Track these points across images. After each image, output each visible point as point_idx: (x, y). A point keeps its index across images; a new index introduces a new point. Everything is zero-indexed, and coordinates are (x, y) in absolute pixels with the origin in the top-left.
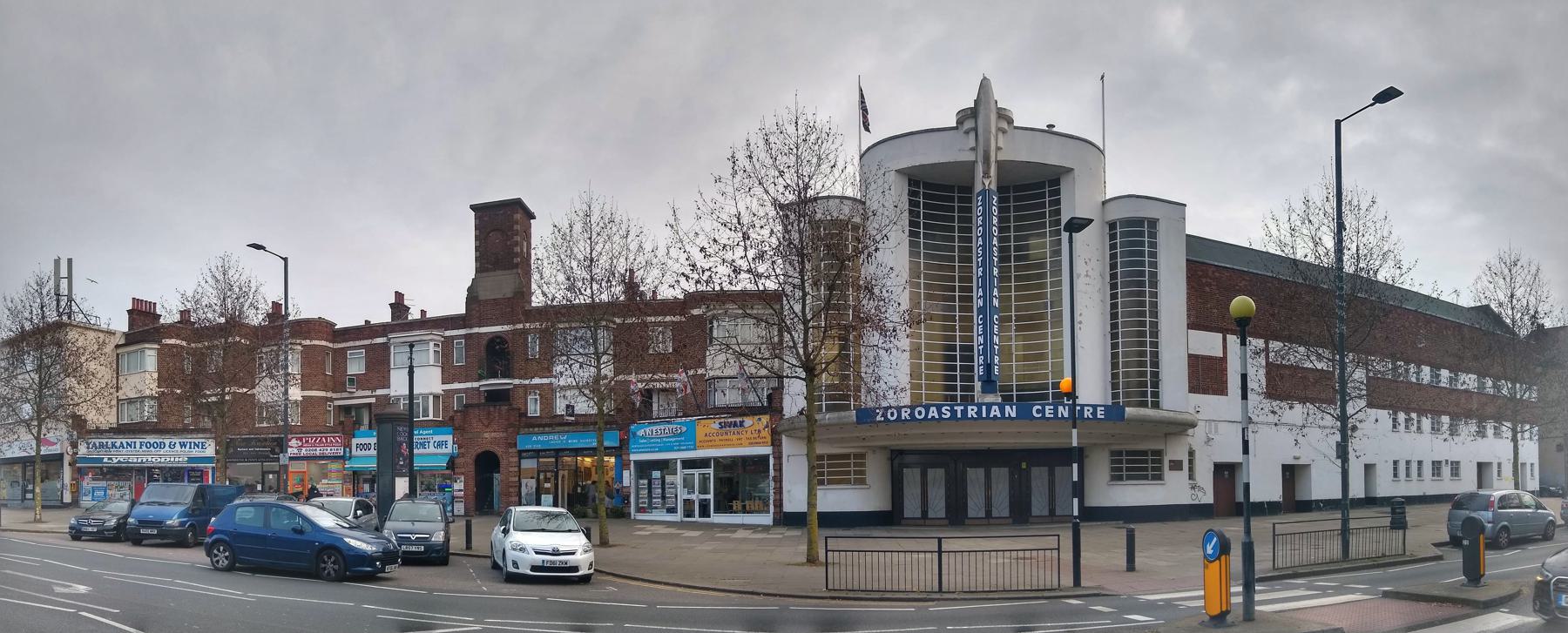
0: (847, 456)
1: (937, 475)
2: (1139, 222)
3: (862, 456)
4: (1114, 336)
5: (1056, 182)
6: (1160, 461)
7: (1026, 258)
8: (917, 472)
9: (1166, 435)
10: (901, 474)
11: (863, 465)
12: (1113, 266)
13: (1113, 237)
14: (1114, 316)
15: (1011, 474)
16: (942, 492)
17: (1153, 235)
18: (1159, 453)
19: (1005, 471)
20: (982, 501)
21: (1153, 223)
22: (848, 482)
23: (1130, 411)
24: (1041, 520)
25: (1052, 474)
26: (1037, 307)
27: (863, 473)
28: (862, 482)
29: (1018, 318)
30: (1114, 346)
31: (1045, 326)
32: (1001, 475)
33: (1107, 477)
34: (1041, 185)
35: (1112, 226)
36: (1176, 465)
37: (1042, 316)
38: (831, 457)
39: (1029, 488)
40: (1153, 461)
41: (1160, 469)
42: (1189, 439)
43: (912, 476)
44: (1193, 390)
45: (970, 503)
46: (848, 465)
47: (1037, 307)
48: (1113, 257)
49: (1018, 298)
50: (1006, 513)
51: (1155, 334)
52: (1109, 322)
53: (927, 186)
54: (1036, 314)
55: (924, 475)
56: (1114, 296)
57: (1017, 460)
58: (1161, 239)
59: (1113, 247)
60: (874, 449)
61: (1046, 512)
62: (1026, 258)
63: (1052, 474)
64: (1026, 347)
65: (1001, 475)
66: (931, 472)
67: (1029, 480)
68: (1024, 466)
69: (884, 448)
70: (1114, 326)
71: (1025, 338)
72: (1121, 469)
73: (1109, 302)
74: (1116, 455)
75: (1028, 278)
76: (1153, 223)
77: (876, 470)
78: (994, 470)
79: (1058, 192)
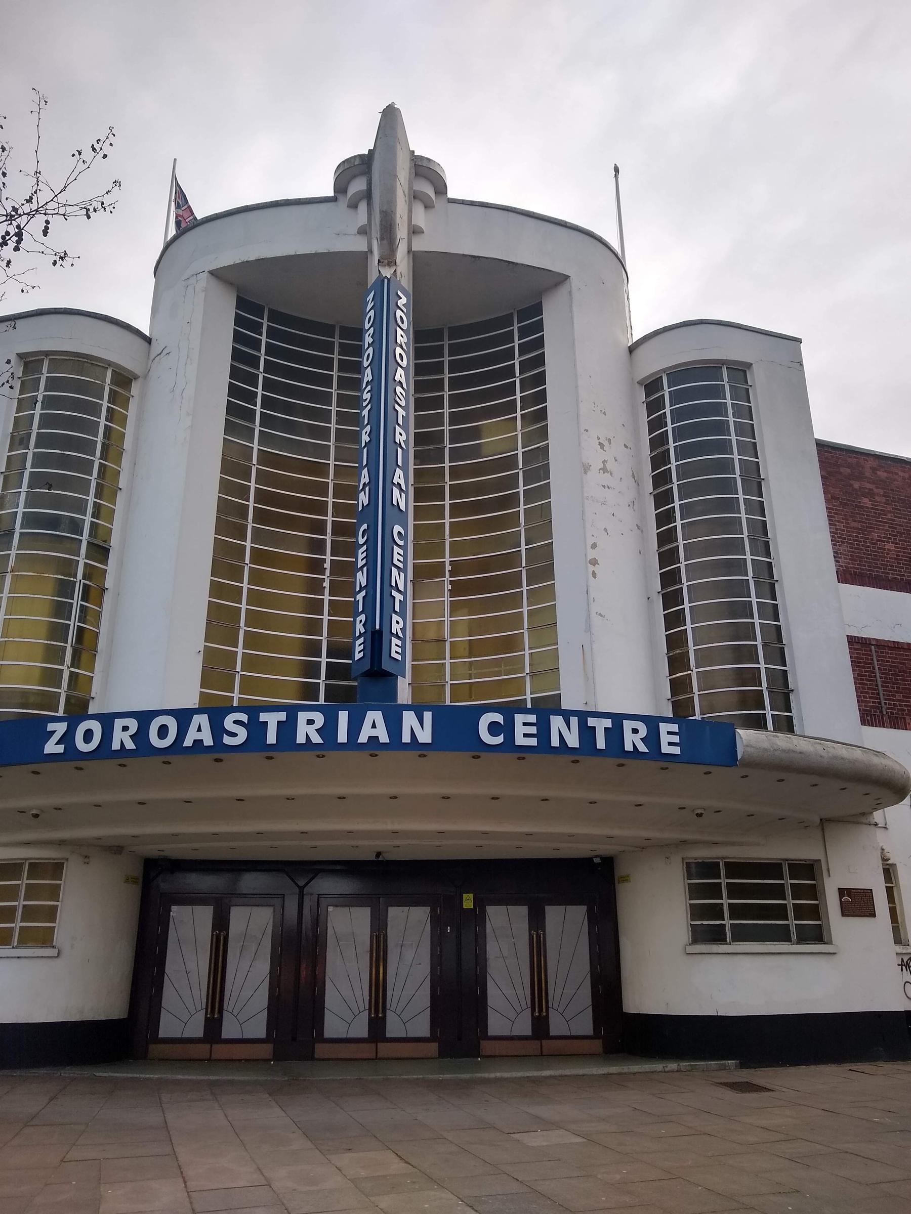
2: (711, 368)
4: (671, 599)
6: (814, 892)
7: (476, 451)
8: (204, 915)
9: (824, 822)
10: (164, 921)
11: (54, 893)
12: (659, 460)
13: (654, 406)
14: (667, 557)
15: (436, 921)
16: (263, 967)
17: (743, 393)
18: (809, 870)
19: (420, 915)
20: (361, 994)
21: (740, 371)
23: (745, 736)
24: (518, 1050)
25: (537, 921)
26: (499, 542)
27: (51, 914)
28: (45, 939)
29: (456, 569)
30: (674, 620)
32: (411, 925)
34: (506, 321)
35: (652, 386)
36: (857, 903)
37: (512, 560)
39: (481, 960)
40: (798, 891)
41: (815, 912)
42: (881, 838)
44: (871, 716)
45: (332, 1000)
47: (499, 542)
48: (658, 442)
50: (421, 1027)
51: (769, 588)
52: (656, 571)
53: (275, 316)
54: (499, 551)
55: (221, 924)
56: (665, 518)
57: (452, 887)
59: (656, 424)
60: (87, 849)
61: (524, 1027)
62: (476, 451)
63: (537, 921)
64: (473, 628)
65: (411, 925)
67: (480, 940)
68: (468, 901)
69: (115, 849)
70: (669, 579)
71: (471, 607)
73: (653, 531)
75: (480, 488)
76: (740, 371)
78: (396, 914)
79: (539, 326)
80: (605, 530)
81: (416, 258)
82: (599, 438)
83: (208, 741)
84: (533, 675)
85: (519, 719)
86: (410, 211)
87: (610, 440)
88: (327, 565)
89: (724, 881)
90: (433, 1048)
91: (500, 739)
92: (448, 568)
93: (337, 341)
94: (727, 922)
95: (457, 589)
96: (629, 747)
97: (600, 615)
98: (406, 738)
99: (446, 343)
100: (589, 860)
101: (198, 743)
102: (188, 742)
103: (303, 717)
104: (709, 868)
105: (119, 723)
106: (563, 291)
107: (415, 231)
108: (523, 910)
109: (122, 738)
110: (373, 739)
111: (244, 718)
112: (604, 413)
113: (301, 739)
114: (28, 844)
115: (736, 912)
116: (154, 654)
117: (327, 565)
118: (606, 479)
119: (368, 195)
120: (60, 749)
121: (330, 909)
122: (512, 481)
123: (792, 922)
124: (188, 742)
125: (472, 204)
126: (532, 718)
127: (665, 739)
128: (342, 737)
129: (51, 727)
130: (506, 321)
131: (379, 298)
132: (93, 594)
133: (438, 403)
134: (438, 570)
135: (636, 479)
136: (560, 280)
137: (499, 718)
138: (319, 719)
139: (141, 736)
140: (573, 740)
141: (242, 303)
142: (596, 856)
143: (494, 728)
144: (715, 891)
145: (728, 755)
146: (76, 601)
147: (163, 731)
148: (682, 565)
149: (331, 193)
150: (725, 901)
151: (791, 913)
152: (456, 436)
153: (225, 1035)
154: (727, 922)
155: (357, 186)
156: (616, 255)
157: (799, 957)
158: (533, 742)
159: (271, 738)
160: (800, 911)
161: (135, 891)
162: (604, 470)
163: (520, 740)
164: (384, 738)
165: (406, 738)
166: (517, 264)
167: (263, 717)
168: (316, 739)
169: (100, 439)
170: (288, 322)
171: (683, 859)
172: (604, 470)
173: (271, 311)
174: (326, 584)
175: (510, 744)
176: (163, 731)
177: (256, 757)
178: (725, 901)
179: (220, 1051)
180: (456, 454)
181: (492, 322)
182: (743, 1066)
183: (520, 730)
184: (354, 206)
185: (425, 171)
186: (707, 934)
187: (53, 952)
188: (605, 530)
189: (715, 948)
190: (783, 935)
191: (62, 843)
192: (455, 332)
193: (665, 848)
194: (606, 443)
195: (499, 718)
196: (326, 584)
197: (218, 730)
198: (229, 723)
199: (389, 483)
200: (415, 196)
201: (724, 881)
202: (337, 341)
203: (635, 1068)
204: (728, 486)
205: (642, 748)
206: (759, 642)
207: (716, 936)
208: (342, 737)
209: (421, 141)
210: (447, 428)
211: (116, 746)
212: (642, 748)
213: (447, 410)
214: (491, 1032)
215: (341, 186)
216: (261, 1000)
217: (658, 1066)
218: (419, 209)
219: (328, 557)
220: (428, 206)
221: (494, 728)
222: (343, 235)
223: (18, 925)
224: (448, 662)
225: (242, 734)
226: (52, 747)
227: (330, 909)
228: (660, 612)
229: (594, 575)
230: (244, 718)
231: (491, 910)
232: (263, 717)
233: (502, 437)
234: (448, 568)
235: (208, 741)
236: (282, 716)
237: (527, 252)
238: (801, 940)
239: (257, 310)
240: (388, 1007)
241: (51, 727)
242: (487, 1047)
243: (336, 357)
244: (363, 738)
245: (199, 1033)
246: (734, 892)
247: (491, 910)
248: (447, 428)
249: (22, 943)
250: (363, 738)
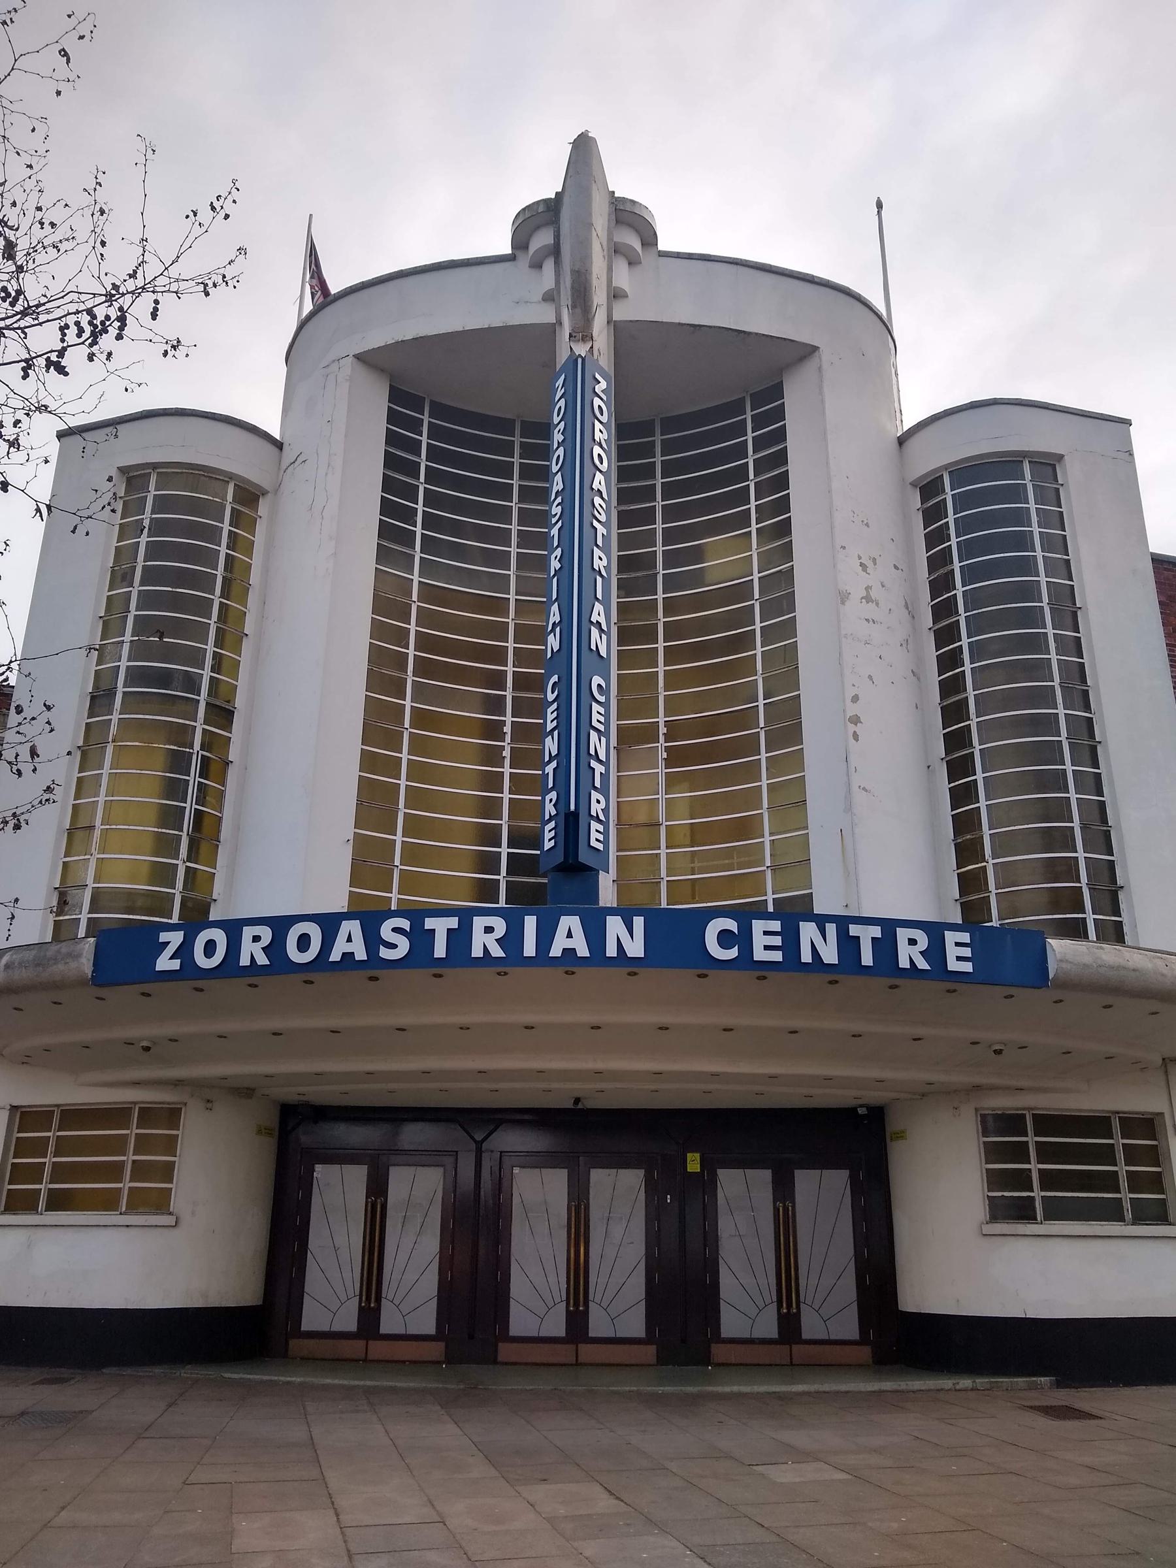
0: (115, 1115)
2: (1009, 463)
4: (959, 767)
7: (697, 578)
8: (356, 1176)
10: (307, 1184)
11: (170, 1145)
12: (940, 585)
13: (933, 514)
14: (953, 712)
15: (651, 1187)
16: (431, 1244)
17: (1051, 495)
19: (632, 1180)
20: (557, 1283)
21: (1048, 465)
22: (107, 1202)
23: (1059, 948)
25: (783, 1190)
26: (729, 696)
27: (167, 1172)
28: (159, 1203)
30: (962, 795)
31: (752, 746)
33: (980, 1210)
34: (736, 407)
35: (929, 488)
37: (746, 719)
38: (73, 1116)
39: (710, 1239)
40: (1132, 1155)
43: (338, 1192)
45: (519, 1288)
46: (119, 1145)
47: (729, 696)
49: (672, 680)
50: (635, 1324)
51: (1089, 751)
52: (938, 732)
53: (438, 410)
54: (731, 709)
55: (377, 1189)
56: (949, 661)
57: (673, 1144)
58: (1074, 504)
59: (935, 538)
60: (210, 1092)
61: (768, 1327)
62: (697, 578)
63: (783, 1190)
67: (709, 1214)
68: (693, 1163)
69: (243, 1092)
70: (956, 741)
71: (692, 780)
72: (1022, 1180)
73: (933, 678)
74: (1004, 1133)
76: (1048, 465)
78: (599, 1177)
79: (779, 414)
80: (870, 677)
81: (621, 332)
82: (860, 558)
83: (361, 955)
84: (774, 869)
85: (758, 926)
86: (610, 269)
87: (874, 561)
88: (507, 729)
89: (1031, 1139)
90: (652, 1349)
91: (733, 953)
92: (663, 730)
93: (517, 440)
94: (1037, 1194)
95: (675, 757)
96: (904, 963)
97: (864, 789)
98: (611, 951)
99: (658, 439)
100: (853, 1110)
101: (348, 956)
102: (335, 956)
103: (479, 923)
104: (1011, 1122)
105: (248, 932)
106: (810, 367)
107: (616, 295)
108: (767, 1174)
109: (252, 951)
110: (569, 952)
111: (405, 924)
112: (867, 525)
113: (477, 952)
114: (136, 1084)
115: (1049, 1180)
116: (292, 846)
117: (507, 729)
118: (869, 610)
119: (555, 251)
120: (176, 965)
121: (516, 1170)
122: (746, 616)
123: (1126, 1196)
124: (335, 956)
125: (690, 257)
126: (776, 926)
127: (952, 952)
128: (530, 949)
129: (164, 937)
130: (736, 407)
131: (570, 384)
132: (213, 768)
133: (648, 516)
134: (650, 734)
135: (910, 609)
136: (809, 351)
137: (731, 925)
138: (500, 926)
139: (275, 949)
140: (830, 955)
141: (396, 395)
142: (861, 1106)
143: (725, 938)
144: (1020, 1152)
145: (1036, 971)
146: (193, 778)
147: (304, 942)
148: (973, 722)
149: (507, 250)
150: (1034, 1166)
151: (1124, 1184)
152: (671, 559)
153: (383, 1330)
154: (1037, 1194)
155: (543, 239)
156: (880, 317)
158: (777, 956)
159: (440, 951)
160: (1136, 1183)
161: (269, 1146)
162: (868, 599)
163: (760, 954)
164: (583, 951)
165: (611, 951)
166: (749, 333)
167: (429, 923)
168: (497, 952)
169: (220, 572)
170: (453, 415)
171: (976, 1110)
172: (868, 599)
173: (433, 404)
174: (506, 753)
175: (746, 959)
176: (304, 942)
177: (419, 976)
178: (1034, 1166)
179: (378, 1349)
180: (671, 583)
181: (718, 407)
182: (1059, 1385)
183: (759, 941)
184: (537, 265)
185: (630, 218)
186: (1010, 1208)
187: (170, 1220)
188: (870, 677)
190: (1113, 1212)
191: (177, 1083)
192: (670, 424)
193: (953, 1095)
194: (869, 564)
195: (731, 925)
196: (506, 753)
197: (373, 940)
198: (386, 931)
199: (585, 622)
200: (616, 250)
201: (1031, 1139)
202: (517, 440)
203: (917, 1384)
204: (1032, 617)
205: (922, 964)
206: (1076, 824)
207: (1023, 1212)
208: (530, 949)
209: (623, 179)
210: (659, 549)
211: (245, 961)
212: (922, 964)
213: (659, 526)
214: (726, 1332)
215: (520, 241)
216: (429, 1284)
217: (946, 1383)
218: (621, 266)
219: (509, 719)
220: (633, 262)
221: (725, 938)
222: (523, 303)
223: (126, 1185)
224: (663, 852)
225: (403, 946)
227: (516, 1170)
228: (943, 785)
229: (856, 737)
230: (405, 924)
231: (723, 1174)
232: (429, 923)
233: (732, 559)
234: (663, 730)
235: (361, 955)
236: (453, 922)
237: (762, 317)
238: (1138, 1220)
239: (416, 403)
240: (591, 1298)
241: (164, 937)
242: (719, 1352)
243: (516, 460)
244: (556, 951)
245: (353, 1327)
246: (1045, 1153)
247: (723, 1174)
248: (659, 549)
249: (132, 1208)
250: (556, 951)
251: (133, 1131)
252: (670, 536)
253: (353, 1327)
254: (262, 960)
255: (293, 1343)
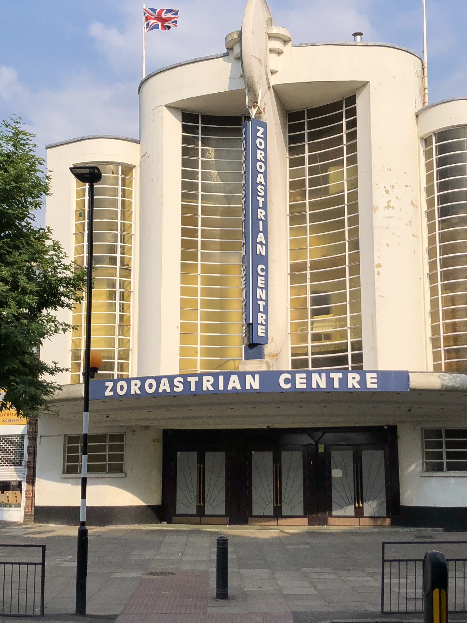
1: (216, 461)
3: (121, 437)
5: (352, 100)
11: (121, 448)
28: (119, 469)
34: (337, 106)
66: (209, 456)
77: (144, 457)
80: (387, 245)
82: (385, 187)
83: (168, 390)
87: (393, 187)
89: (444, 440)
92: (309, 265)
94: (445, 461)
97: (382, 296)
99: (306, 120)
100: (382, 427)
104: (438, 433)
105: (133, 382)
106: (365, 91)
111: (181, 379)
112: (390, 170)
115: (450, 455)
120: (111, 394)
121: (253, 452)
127: (369, 381)
129: (107, 384)
132: (125, 296)
137: (289, 376)
139: (142, 388)
142: (385, 425)
143: (287, 381)
146: (118, 301)
147: (151, 386)
152: (313, 182)
153: (206, 513)
157: (462, 479)
159: (193, 389)
162: (388, 207)
166: (334, 82)
167: (189, 379)
169: (119, 209)
171: (422, 428)
172: (388, 207)
176: (151, 386)
187: (123, 475)
188: (387, 245)
189: (435, 474)
192: (313, 112)
194: (390, 189)
195: (289, 376)
198: (176, 382)
201: (444, 440)
207: (439, 468)
211: (133, 392)
213: (307, 166)
221: (287, 381)
223: (107, 463)
226: (108, 393)
227: (253, 452)
229: (379, 273)
230: (181, 379)
240: (283, 501)
241: (107, 384)
245: (195, 512)
246: (449, 445)
251: (108, 443)
252: (312, 171)
253: (195, 512)
254: (138, 392)
255: (174, 518)
